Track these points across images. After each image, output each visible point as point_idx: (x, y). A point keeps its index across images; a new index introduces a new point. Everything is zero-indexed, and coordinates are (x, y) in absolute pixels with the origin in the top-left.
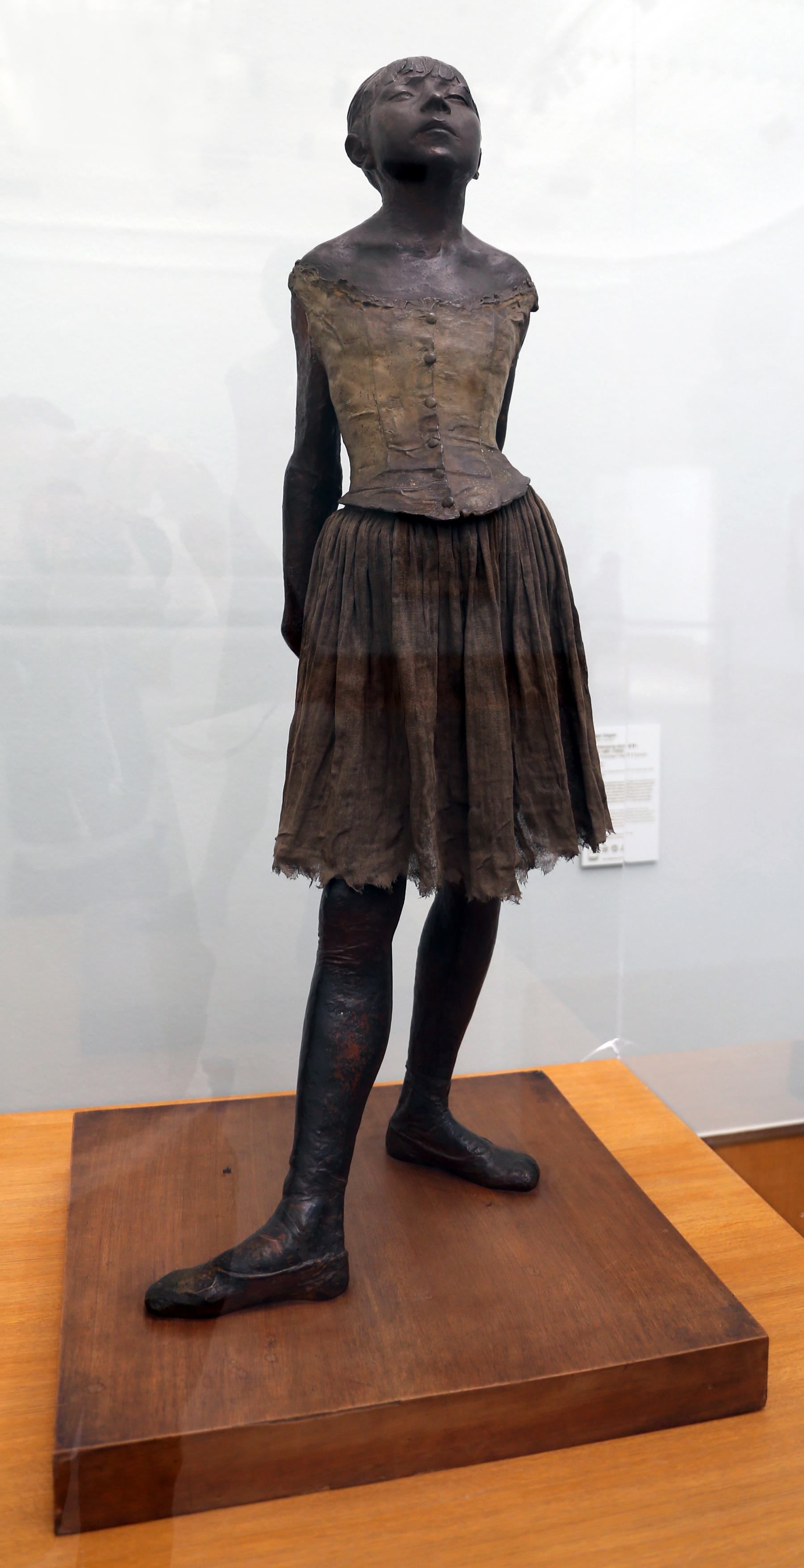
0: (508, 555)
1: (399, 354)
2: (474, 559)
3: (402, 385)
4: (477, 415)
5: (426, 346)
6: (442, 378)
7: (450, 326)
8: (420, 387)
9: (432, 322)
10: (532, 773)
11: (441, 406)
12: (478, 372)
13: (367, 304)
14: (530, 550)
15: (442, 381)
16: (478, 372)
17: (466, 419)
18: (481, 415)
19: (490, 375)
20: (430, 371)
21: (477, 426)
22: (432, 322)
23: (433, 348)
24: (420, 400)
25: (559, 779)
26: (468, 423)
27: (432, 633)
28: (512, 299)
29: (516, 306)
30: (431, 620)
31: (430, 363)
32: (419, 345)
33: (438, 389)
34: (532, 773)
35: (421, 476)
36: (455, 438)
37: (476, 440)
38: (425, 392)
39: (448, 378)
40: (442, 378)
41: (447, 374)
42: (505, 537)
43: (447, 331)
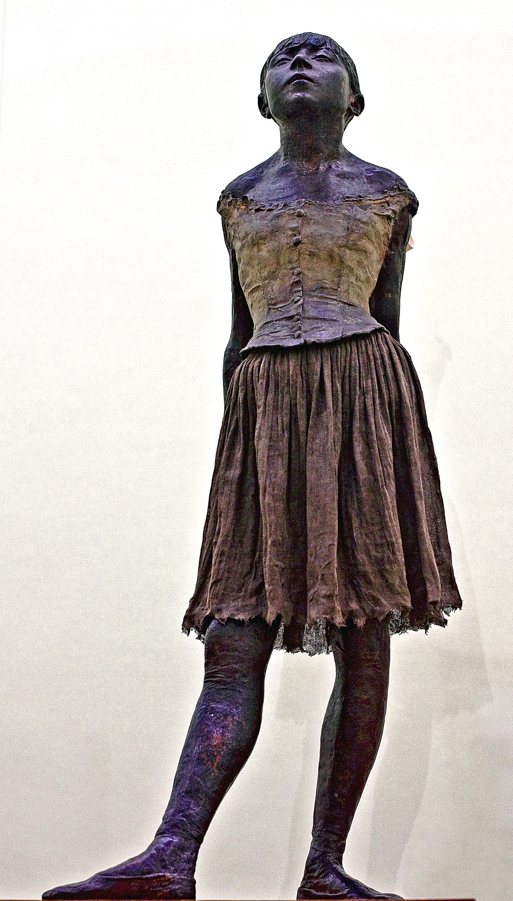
0: (350, 377)
1: (275, 241)
2: (317, 378)
3: (278, 263)
4: (336, 279)
5: (295, 233)
6: (306, 254)
7: (315, 218)
8: (290, 262)
9: (299, 215)
10: (368, 541)
11: (306, 275)
12: (335, 249)
13: (257, 210)
14: (371, 375)
15: (308, 257)
16: (335, 249)
17: (325, 283)
18: (340, 280)
19: (348, 251)
20: (297, 250)
21: (336, 288)
22: (299, 215)
23: (300, 234)
24: (291, 272)
25: (390, 545)
26: (327, 286)
27: (283, 432)
28: (381, 199)
29: (386, 205)
30: (282, 422)
31: (297, 243)
32: (290, 233)
33: (304, 263)
34: (368, 541)
35: (284, 322)
36: (316, 296)
37: (335, 298)
38: (294, 265)
39: (312, 254)
40: (306, 254)
41: (311, 251)
42: (347, 365)
43: (312, 221)
